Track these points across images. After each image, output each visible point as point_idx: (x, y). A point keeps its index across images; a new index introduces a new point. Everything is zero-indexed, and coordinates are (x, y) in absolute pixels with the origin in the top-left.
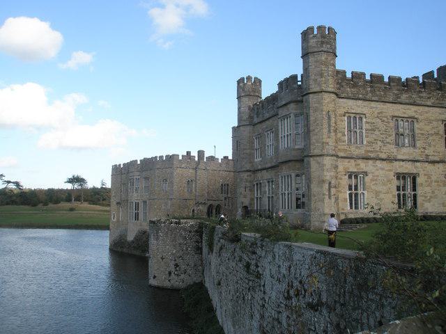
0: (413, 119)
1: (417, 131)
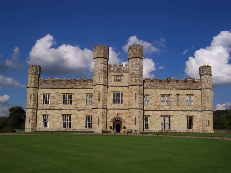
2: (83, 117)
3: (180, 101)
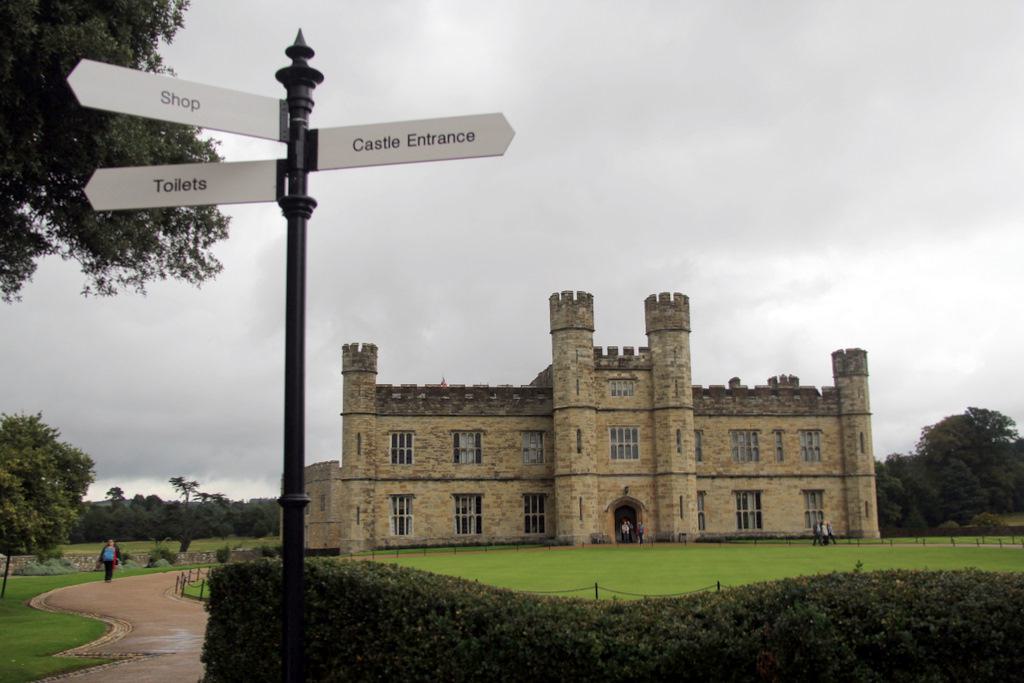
0: (478, 434)
1: (483, 445)
2: (517, 501)
3: (784, 448)
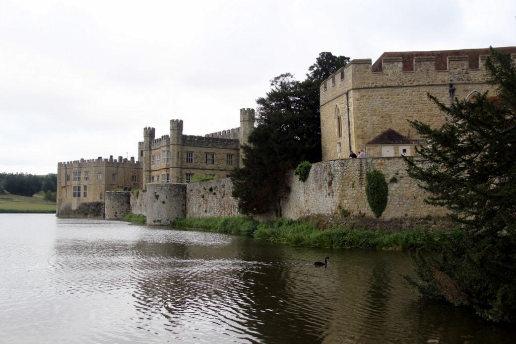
0: (213, 154)
